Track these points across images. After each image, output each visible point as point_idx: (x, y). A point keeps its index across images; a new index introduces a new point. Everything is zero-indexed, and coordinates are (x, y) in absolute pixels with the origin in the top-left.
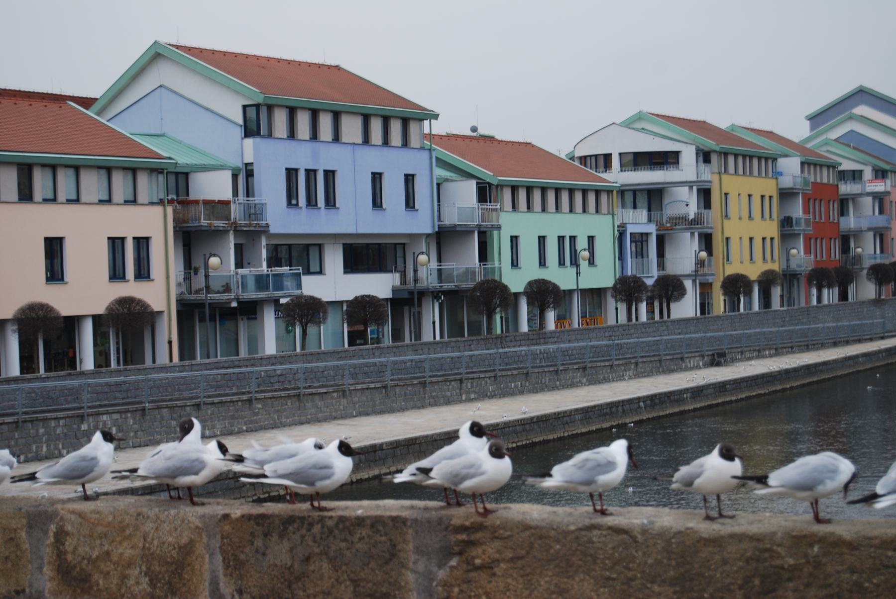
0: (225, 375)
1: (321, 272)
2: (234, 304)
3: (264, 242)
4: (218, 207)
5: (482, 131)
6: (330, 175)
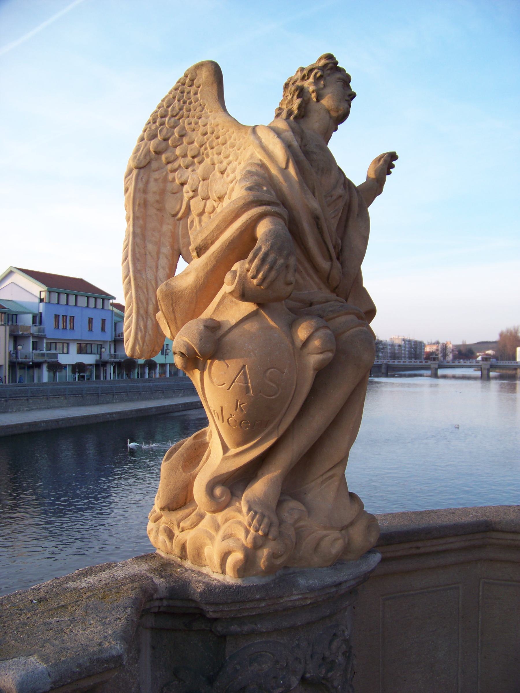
0: (20, 389)
1: (68, 353)
2: (31, 364)
3: (45, 341)
6: (72, 318)
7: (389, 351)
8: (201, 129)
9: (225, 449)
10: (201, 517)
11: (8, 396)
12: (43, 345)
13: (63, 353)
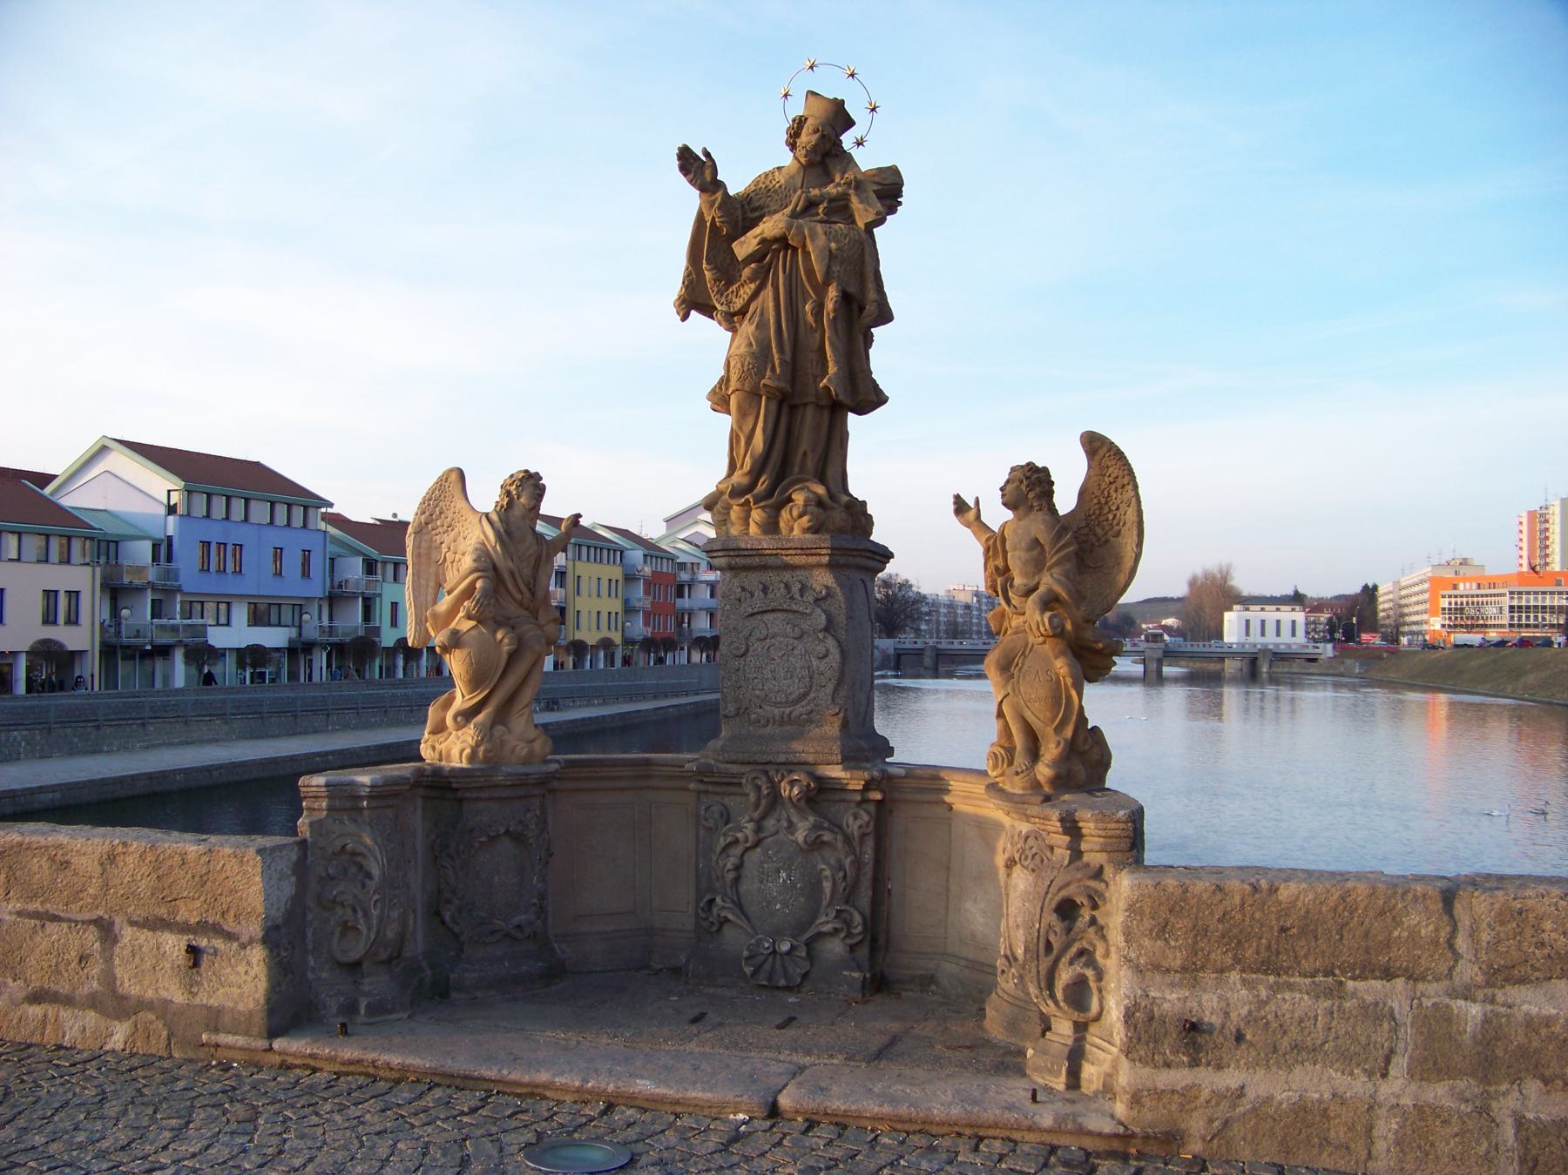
1: (228, 624)
2: (149, 647)
3: (179, 598)
4: (141, 570)
7: (942, 619)
9: (463, 696)
10: (451, 734)
11: (101, 718)
12: (175, 606)
13: (218, 624)
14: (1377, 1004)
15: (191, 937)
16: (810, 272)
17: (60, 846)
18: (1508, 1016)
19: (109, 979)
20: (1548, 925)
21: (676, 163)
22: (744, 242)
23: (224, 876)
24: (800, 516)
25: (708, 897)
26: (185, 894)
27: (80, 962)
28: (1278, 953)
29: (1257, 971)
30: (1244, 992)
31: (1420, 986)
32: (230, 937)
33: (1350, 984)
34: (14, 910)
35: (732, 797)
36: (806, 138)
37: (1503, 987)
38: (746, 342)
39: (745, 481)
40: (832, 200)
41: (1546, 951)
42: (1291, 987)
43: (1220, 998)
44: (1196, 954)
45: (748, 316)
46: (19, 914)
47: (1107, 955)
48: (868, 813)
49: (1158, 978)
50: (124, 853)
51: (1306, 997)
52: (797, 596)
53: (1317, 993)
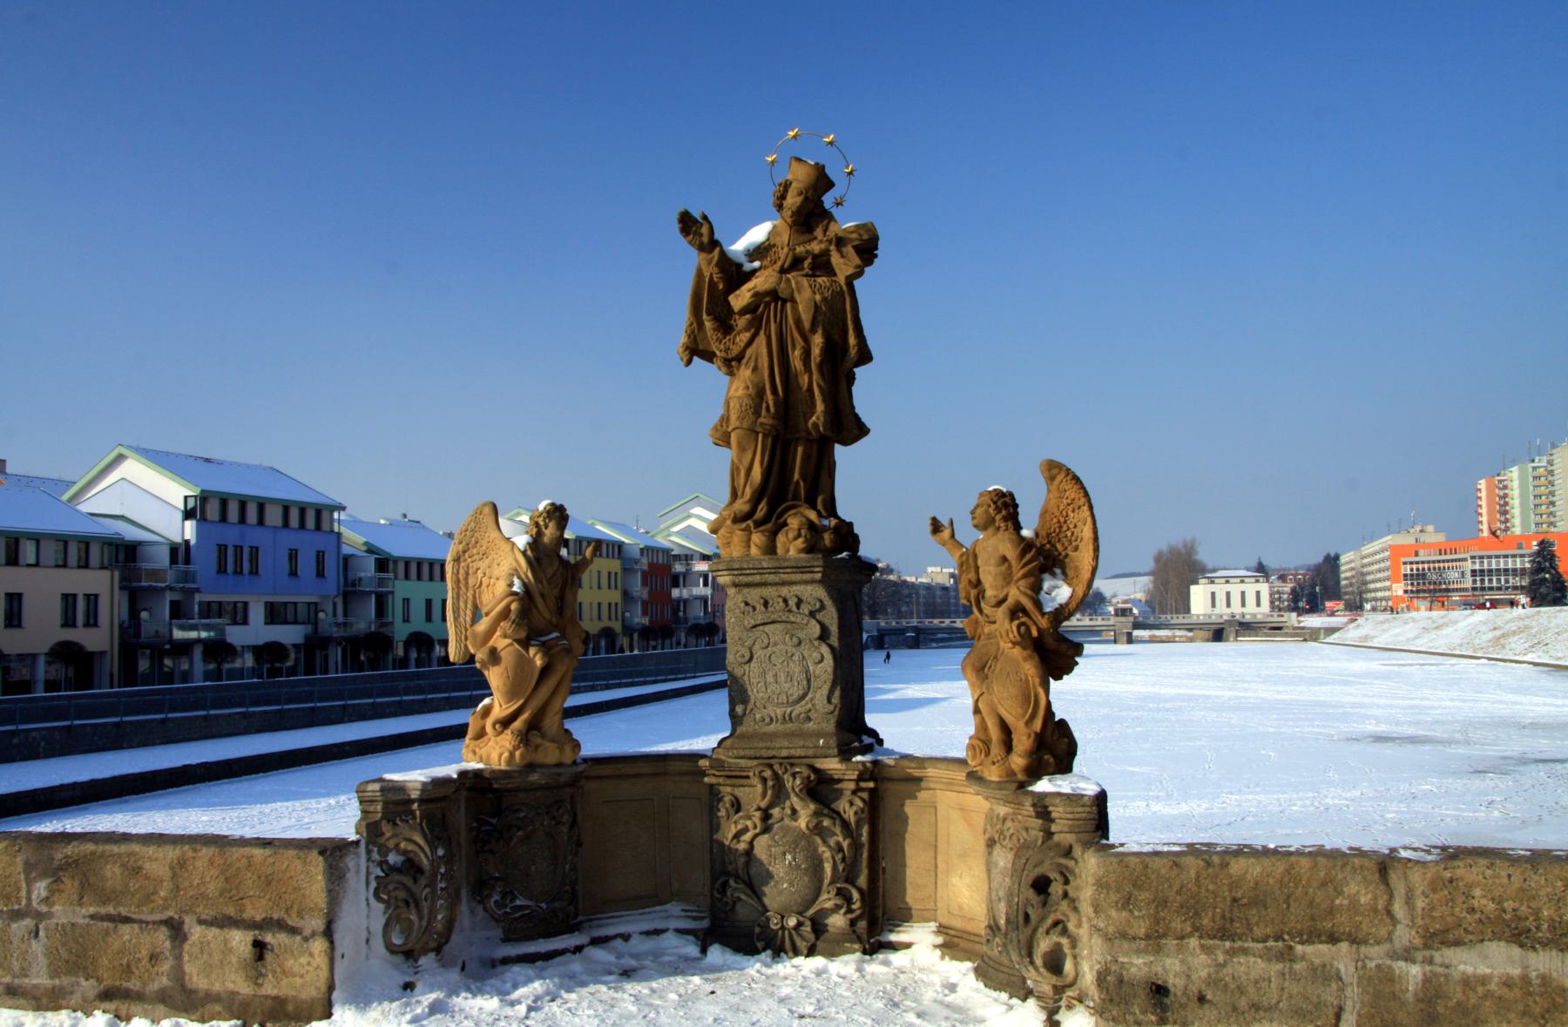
2: (168, 647)
5: (410, 517)
6: (255, 551)
8: (487, 540)
9: (501, 706)
10: (490, 740)
14: (1324, 966)
15: (257, 932)
16: (798, 322)
17: (132, 854)
18: (1446, 976)
19: (179, 975)
20: (1477, 892)
21: (676, 226)
22: (739, 296)
23: (288, 875)
24: (796, 538)
25: (723, 879)
26: (251, 893)
27: (151, 959)
28: (1232, 920)
29: (1214, 937)
30: (1203, 957)
31: (1363, 949)
32: (294, 931)
33: (1299, 948)
34: (87, 914)
35: (742, 789)
36: (792, 200)
37: (1438, 949)
38: (744, 385)
39: (746, 508)
40: (815, 257)
41: (1477, 916)
42: (1245, 951)
43: (1182, 961)
44: (1158, 923)
45: (745, 361)
46: (92, 917)
47: (1079, 925)
48: (863, 800)
49: (1125, 945)
50: (194, 858)
51: (1259, 960)
52: (794, 609)
53: (1268, 956)
